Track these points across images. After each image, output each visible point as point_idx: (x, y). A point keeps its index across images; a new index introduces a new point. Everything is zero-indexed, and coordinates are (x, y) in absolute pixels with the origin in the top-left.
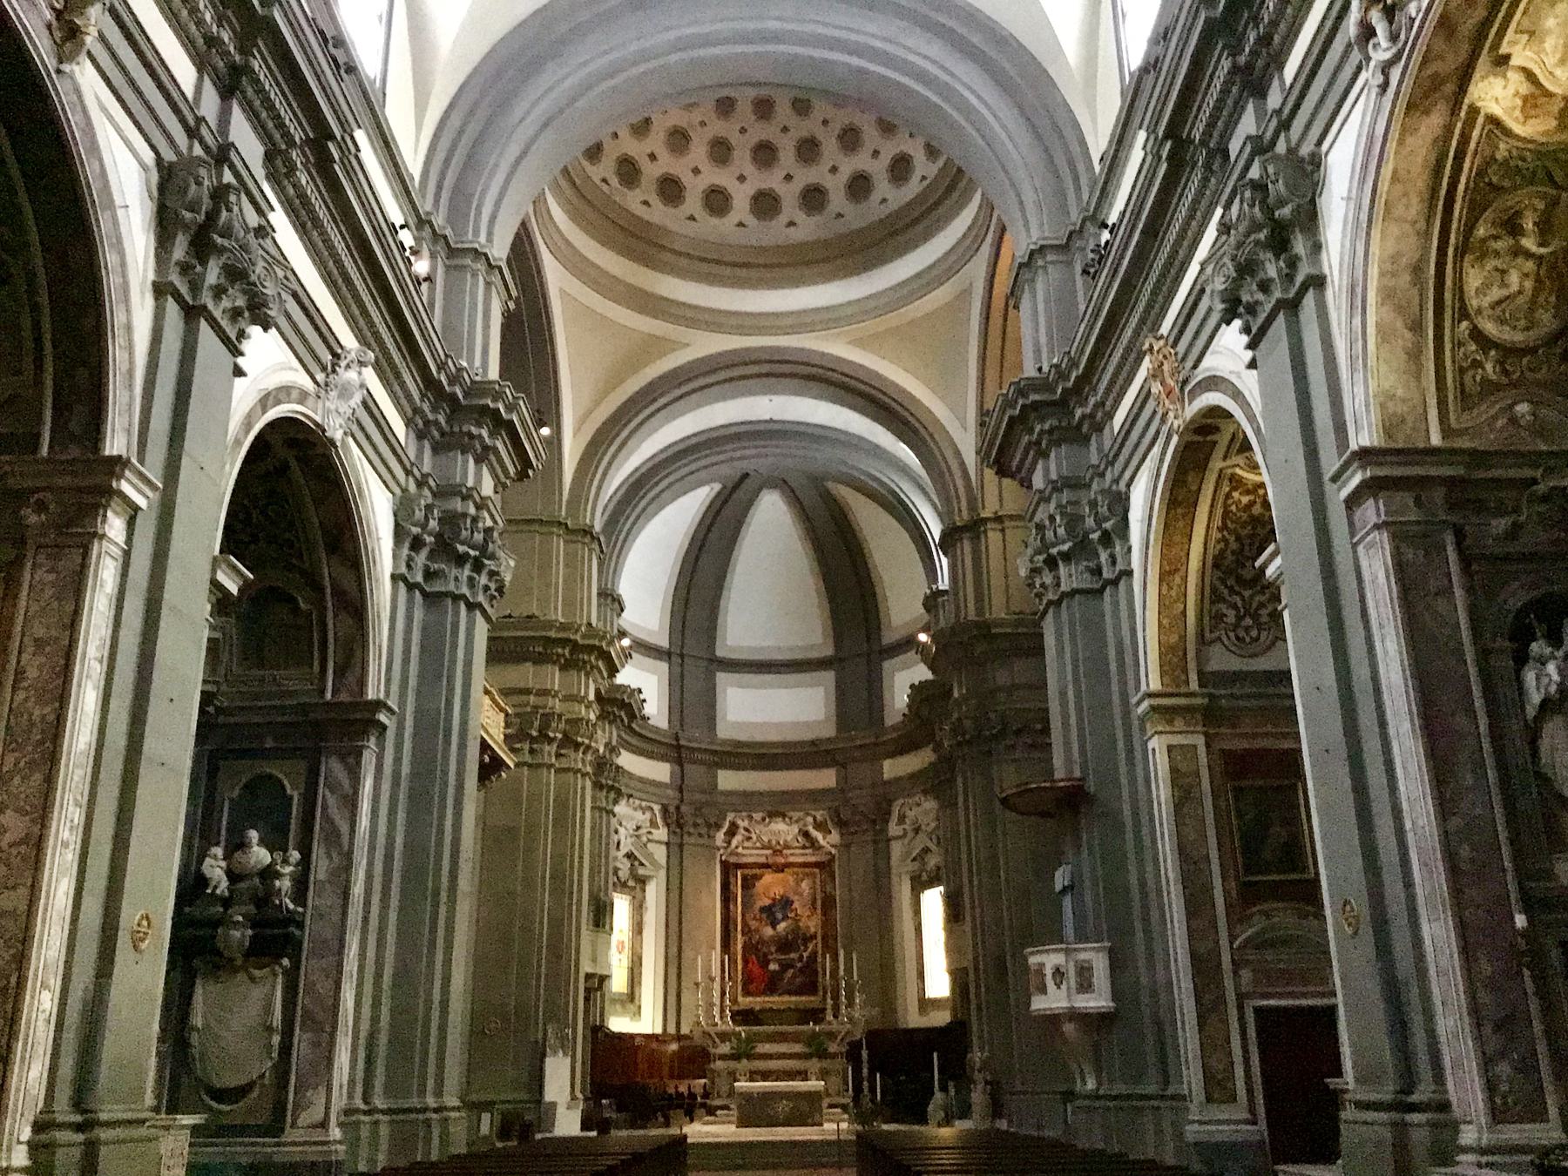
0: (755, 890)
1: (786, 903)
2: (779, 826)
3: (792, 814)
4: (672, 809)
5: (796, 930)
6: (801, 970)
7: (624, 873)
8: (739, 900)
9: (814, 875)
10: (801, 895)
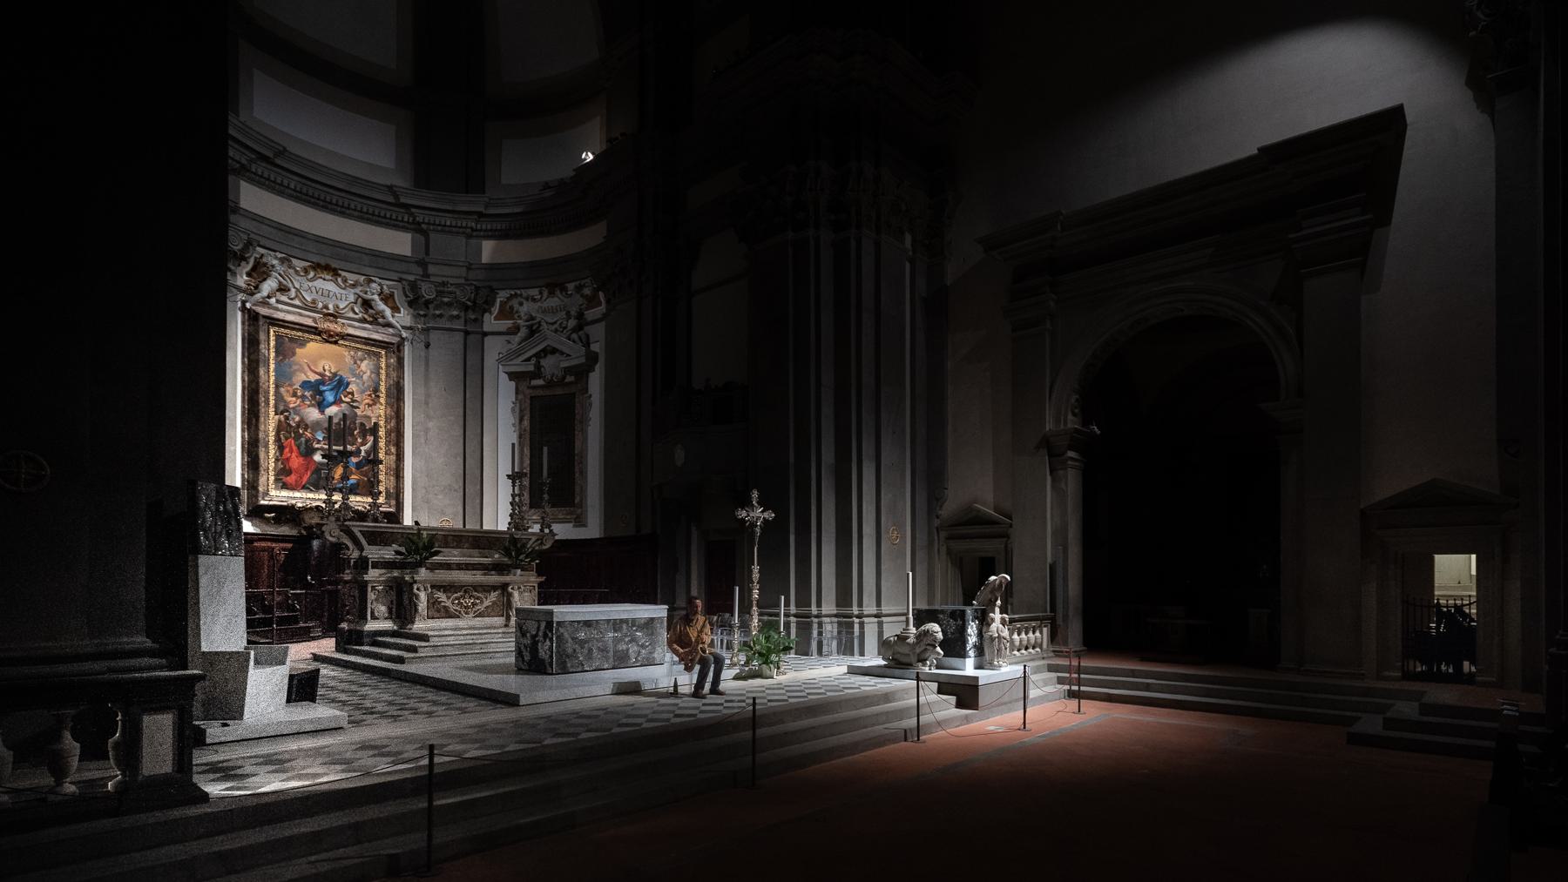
0: (295, 358)
1: (340, 384)
2: (326, 285)
8: (272, 366)
9: (378, 355)
10: (360, 377)
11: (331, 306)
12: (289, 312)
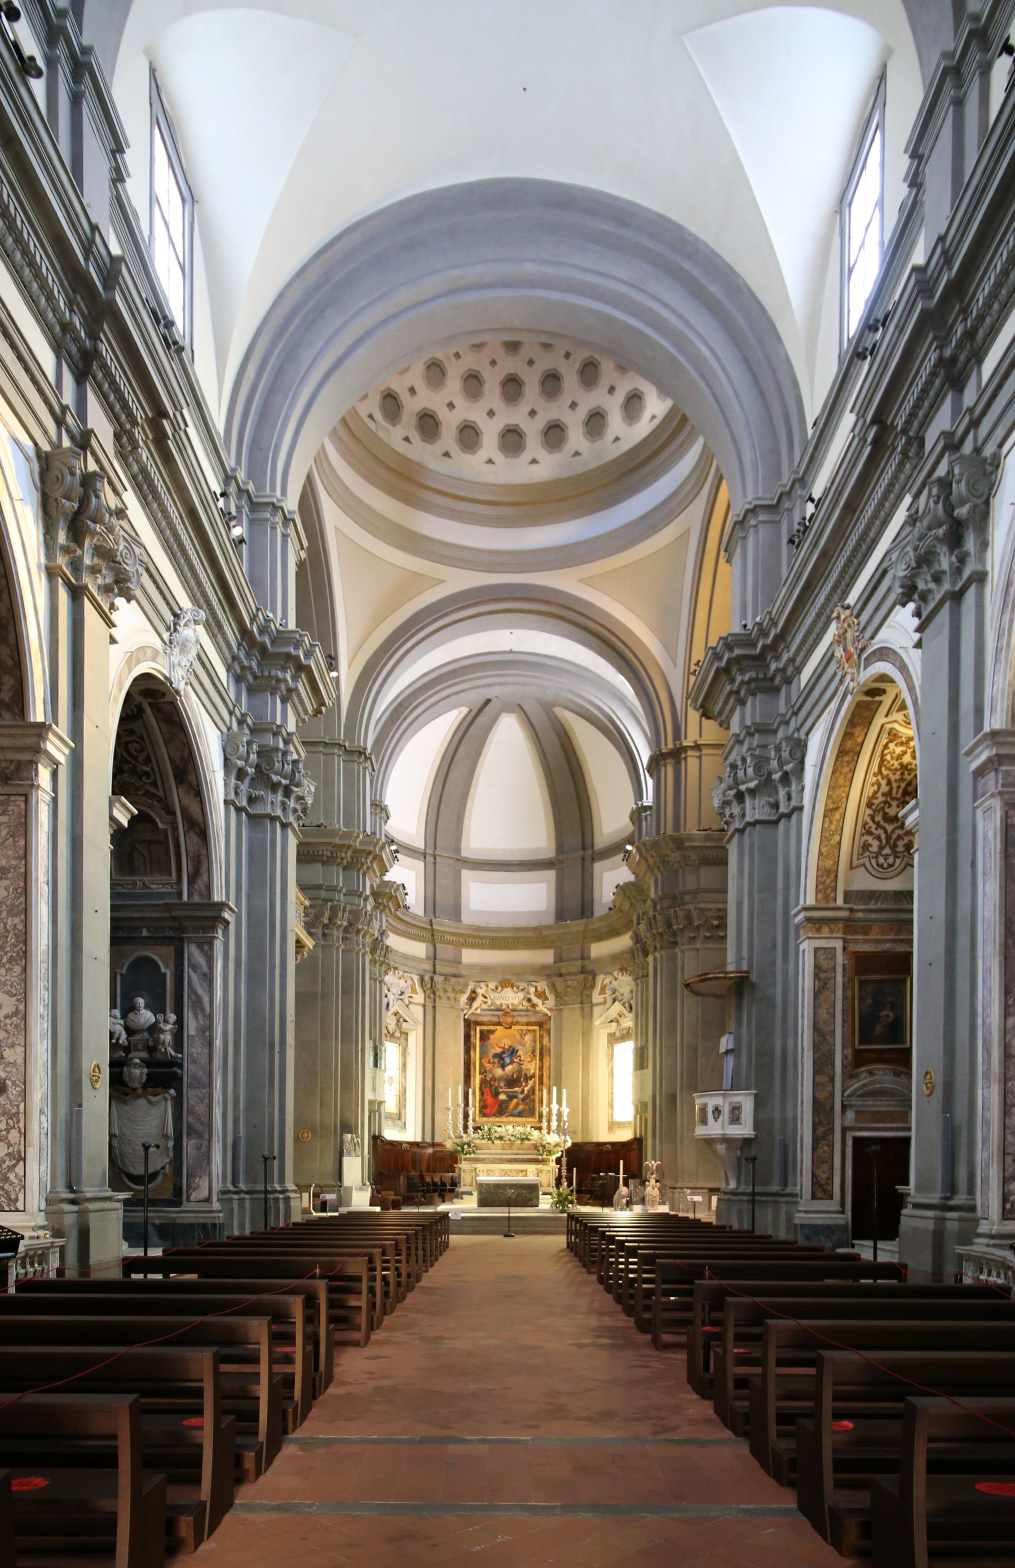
2: (508, 992)
3: (519, 984)
4: (427, 978)
5: (520, 1071)
6: (523, 1100)
7: (392, 1027)
8: (478, 1049)
10: (524, 1045)
11: (510, 1007)
12: (486, 1015)
